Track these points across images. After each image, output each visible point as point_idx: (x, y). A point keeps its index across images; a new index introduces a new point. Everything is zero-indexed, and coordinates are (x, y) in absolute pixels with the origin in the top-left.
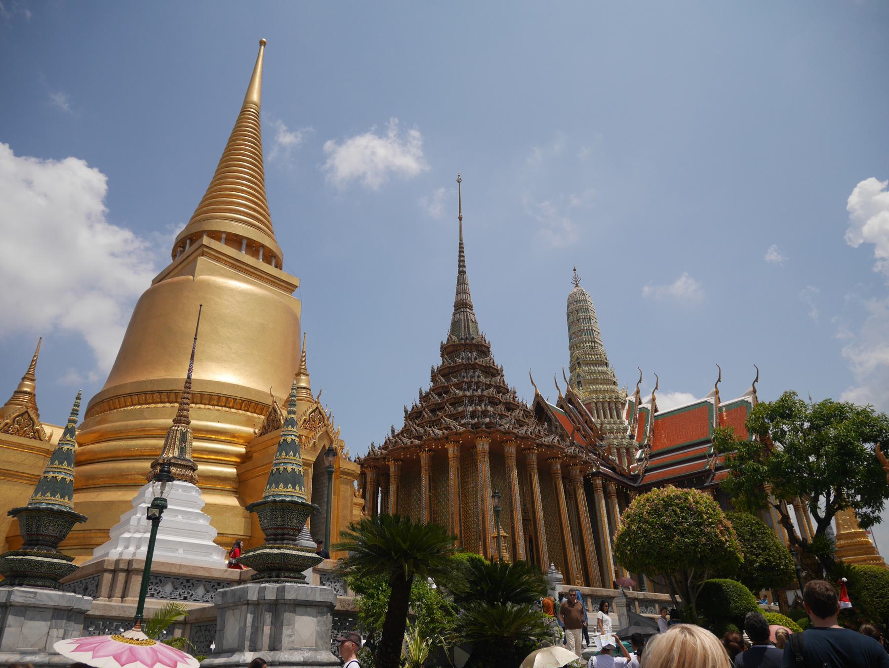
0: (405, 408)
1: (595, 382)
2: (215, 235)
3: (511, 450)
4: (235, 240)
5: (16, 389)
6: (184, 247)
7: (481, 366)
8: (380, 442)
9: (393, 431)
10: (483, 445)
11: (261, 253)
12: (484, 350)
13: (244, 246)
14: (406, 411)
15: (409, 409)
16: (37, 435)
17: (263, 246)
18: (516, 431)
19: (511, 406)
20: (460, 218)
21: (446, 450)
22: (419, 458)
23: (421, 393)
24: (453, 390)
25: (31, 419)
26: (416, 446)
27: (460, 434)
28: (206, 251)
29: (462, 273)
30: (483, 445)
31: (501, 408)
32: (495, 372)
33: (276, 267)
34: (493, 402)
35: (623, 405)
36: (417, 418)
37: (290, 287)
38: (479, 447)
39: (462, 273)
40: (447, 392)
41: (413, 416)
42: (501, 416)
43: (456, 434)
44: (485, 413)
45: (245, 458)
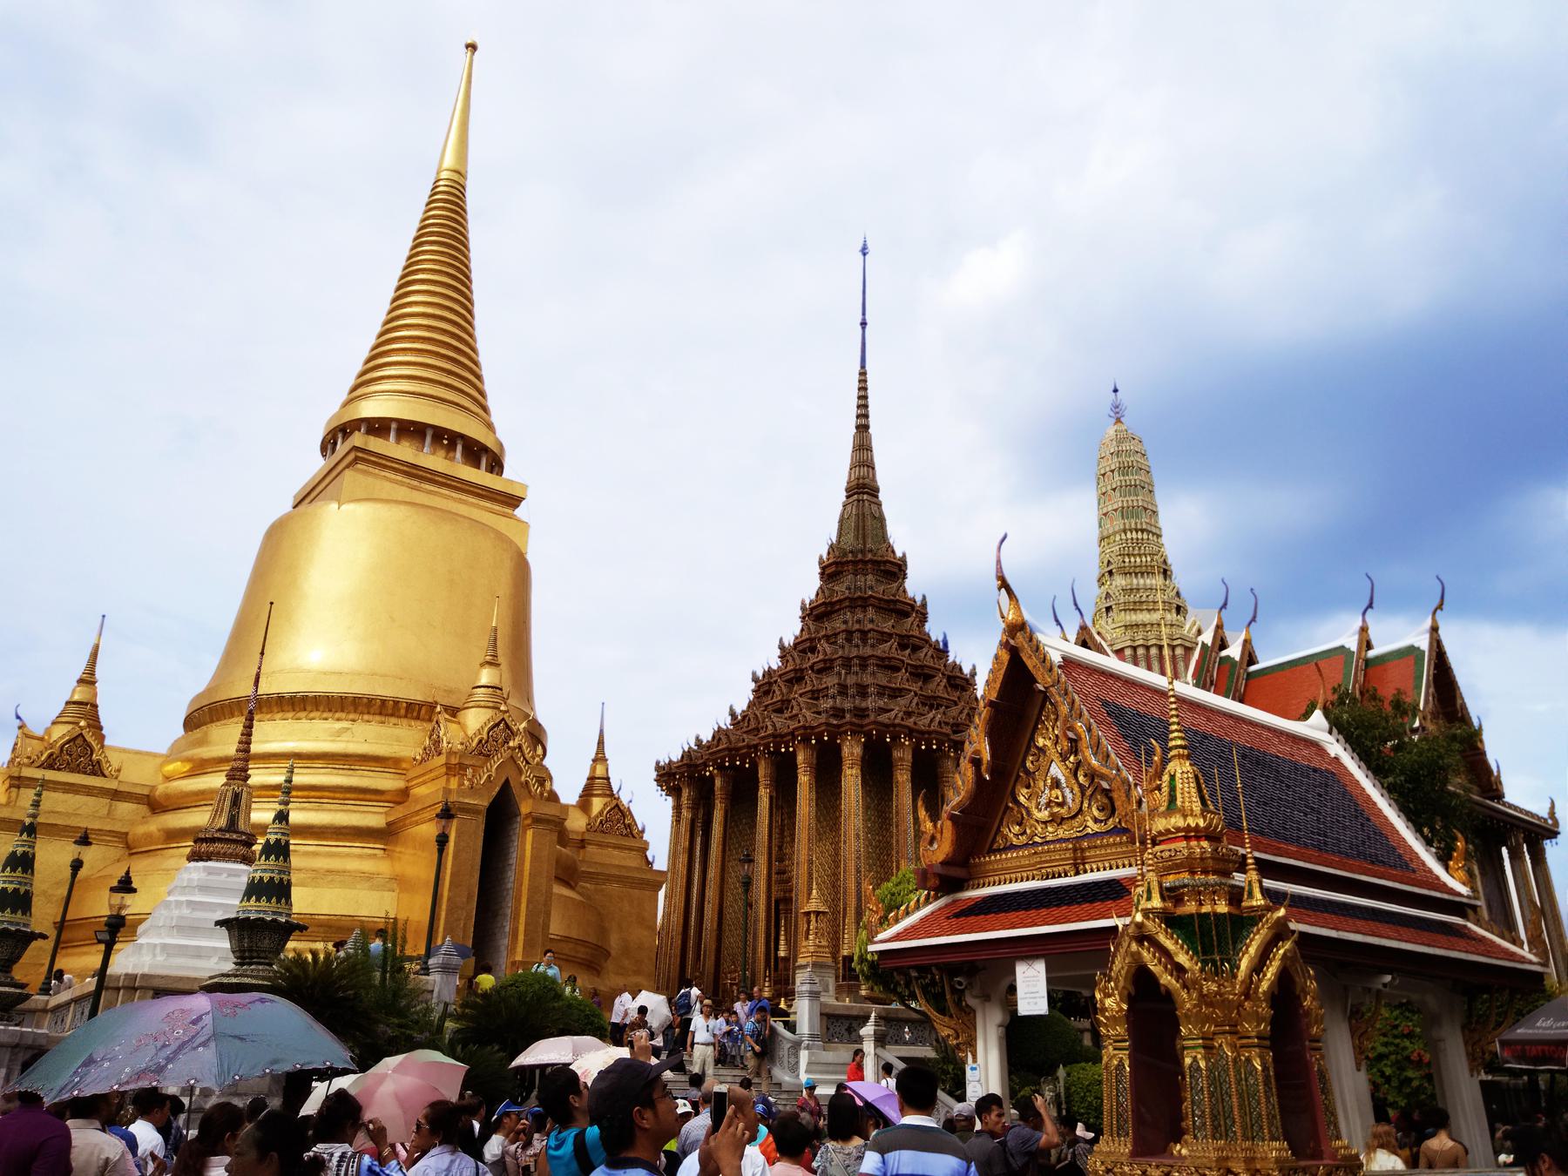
0: (754, 674)
1: (1136, 607)
2: (378, 427)
3: (903, 755)
4: (411, 430)
5: (67, 698)
6: (335, 444)
7: (880, 600)
8: (707, 737)
9: (733, 714)
10: (851, 750)
11: (459, 448)
12: (895, 570)
13: (428, 439)
14: (755, 679)
15: (760, 674)
16: (97, 769)
17: (462, 436)
18: (910, 722)
19: (922, 674)
20: (864, 324)
21: (794, 755)
22: (754, 766)
23: (782, 647)
24: (823, 646)
25: (89, 745)
26: (749, 747)
27: (813, 728)
28: (361, 457)
29: (863, 428)
30: (851, 750)
31: (900, 679)
32: (908, 609)
33: (491, 469)
34: (889, 666)
35: (1189, 650)
36: (767, 693)
37: (513, 501)
38: (846, 751)
39: (863, 428)
40: (813, 650)
41: (764, 686)
42: (896, 693)
43: (804, 727)
44: (862, 691)
45: (403, 796)
